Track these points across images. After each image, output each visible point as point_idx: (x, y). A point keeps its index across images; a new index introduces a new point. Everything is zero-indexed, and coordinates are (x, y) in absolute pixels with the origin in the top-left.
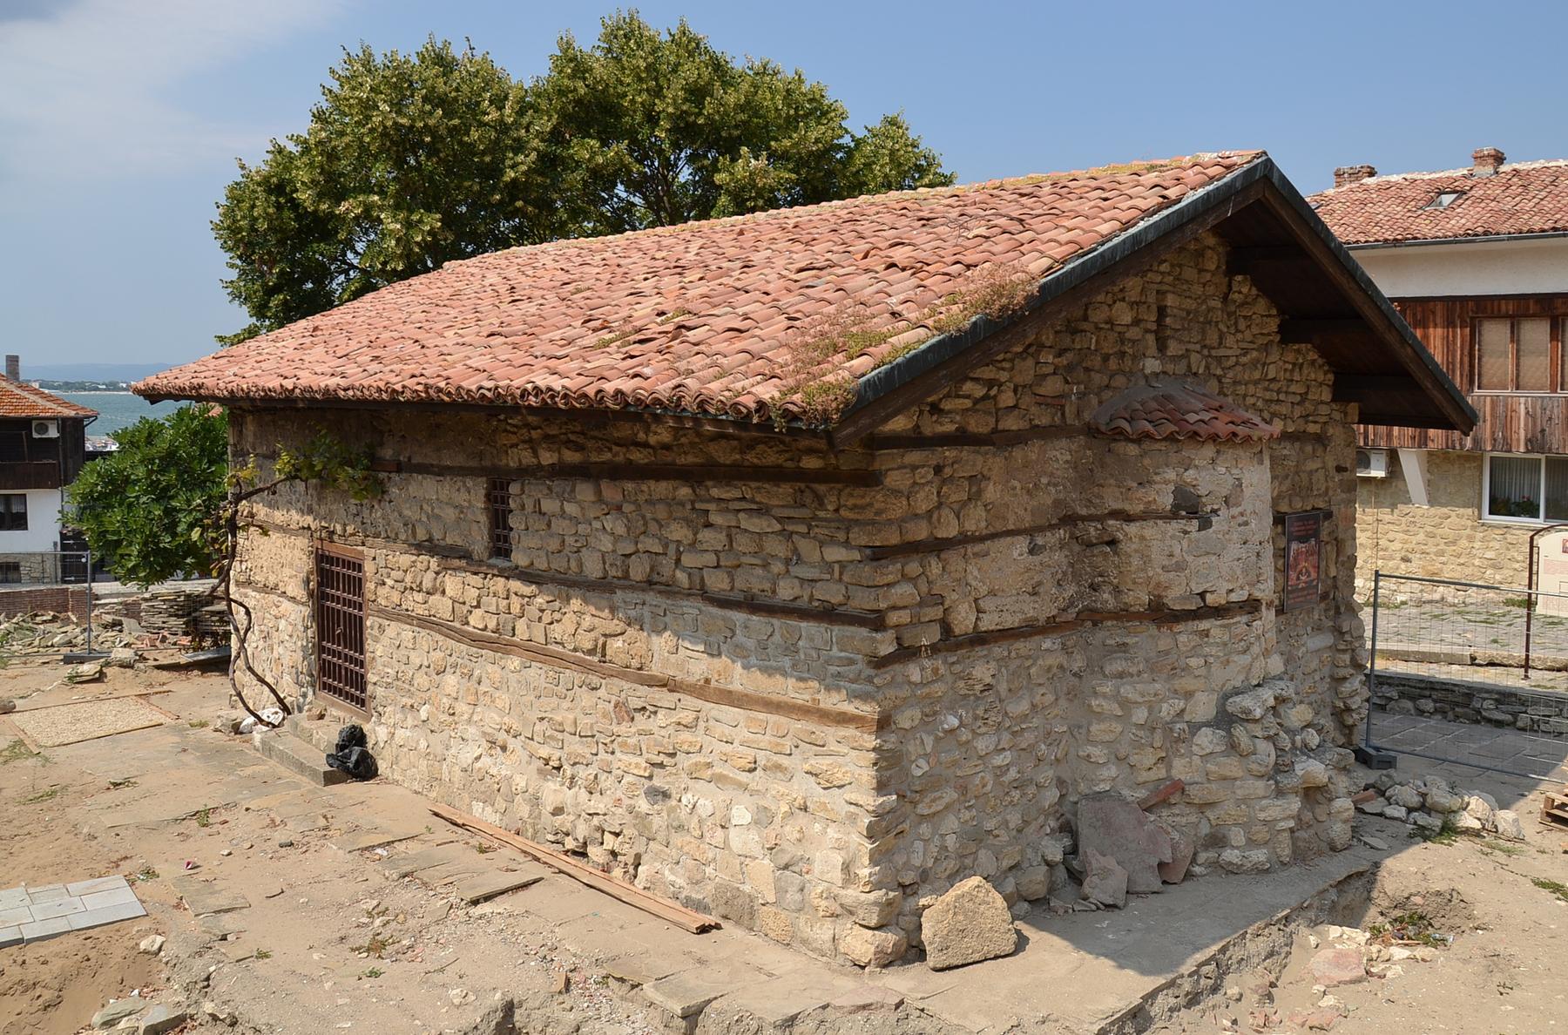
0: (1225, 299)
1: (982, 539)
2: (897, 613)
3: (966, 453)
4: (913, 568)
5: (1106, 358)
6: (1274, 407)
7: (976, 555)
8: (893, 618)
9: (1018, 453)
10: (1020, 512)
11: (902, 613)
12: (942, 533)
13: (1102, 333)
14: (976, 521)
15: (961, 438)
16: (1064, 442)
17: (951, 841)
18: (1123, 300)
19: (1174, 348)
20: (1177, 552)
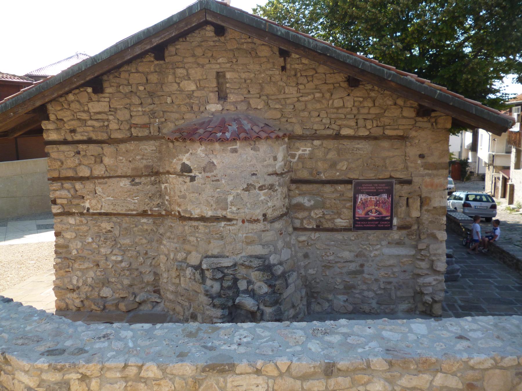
0: (284, 68)
1: (104, 178)
2: (60, 200)
3: (92, 147)
4: (67, 185)
5: (179, 106)
6: (339, 122)
7: (99, 183)
8: (59, 201)
9: (123, 147)
10: (125, 168)
11: (63, 200)
12: (81, 175)
13: (174, 97)
14: (99, 171)
15: (89, 141)
16: (152, 142)
17: (89, 280)
18: (189, 79)
19: (232, 98)
20: (183, 190)
